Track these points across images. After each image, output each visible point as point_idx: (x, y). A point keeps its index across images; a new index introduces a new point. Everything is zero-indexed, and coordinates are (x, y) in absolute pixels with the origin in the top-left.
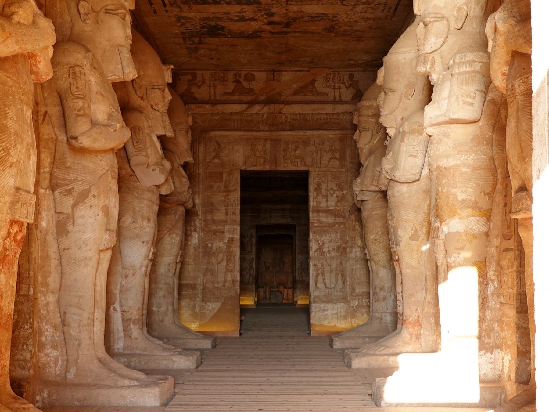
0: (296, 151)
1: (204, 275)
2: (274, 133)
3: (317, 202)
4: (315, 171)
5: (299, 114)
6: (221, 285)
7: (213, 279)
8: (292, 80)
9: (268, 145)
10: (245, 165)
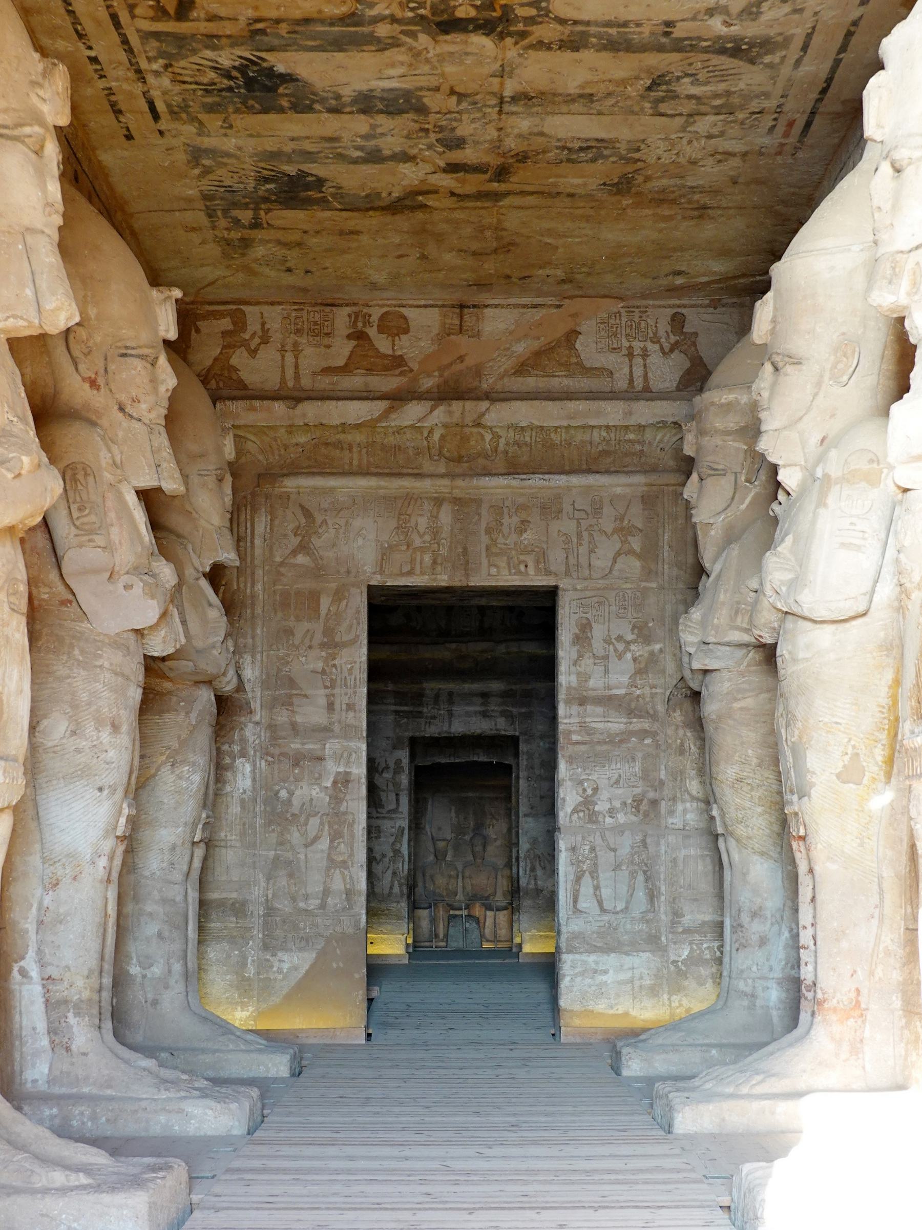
1: (269, 879)
2: (460, 482)
4: (576, 590)
5: (531, 427)
8: (511, 333)
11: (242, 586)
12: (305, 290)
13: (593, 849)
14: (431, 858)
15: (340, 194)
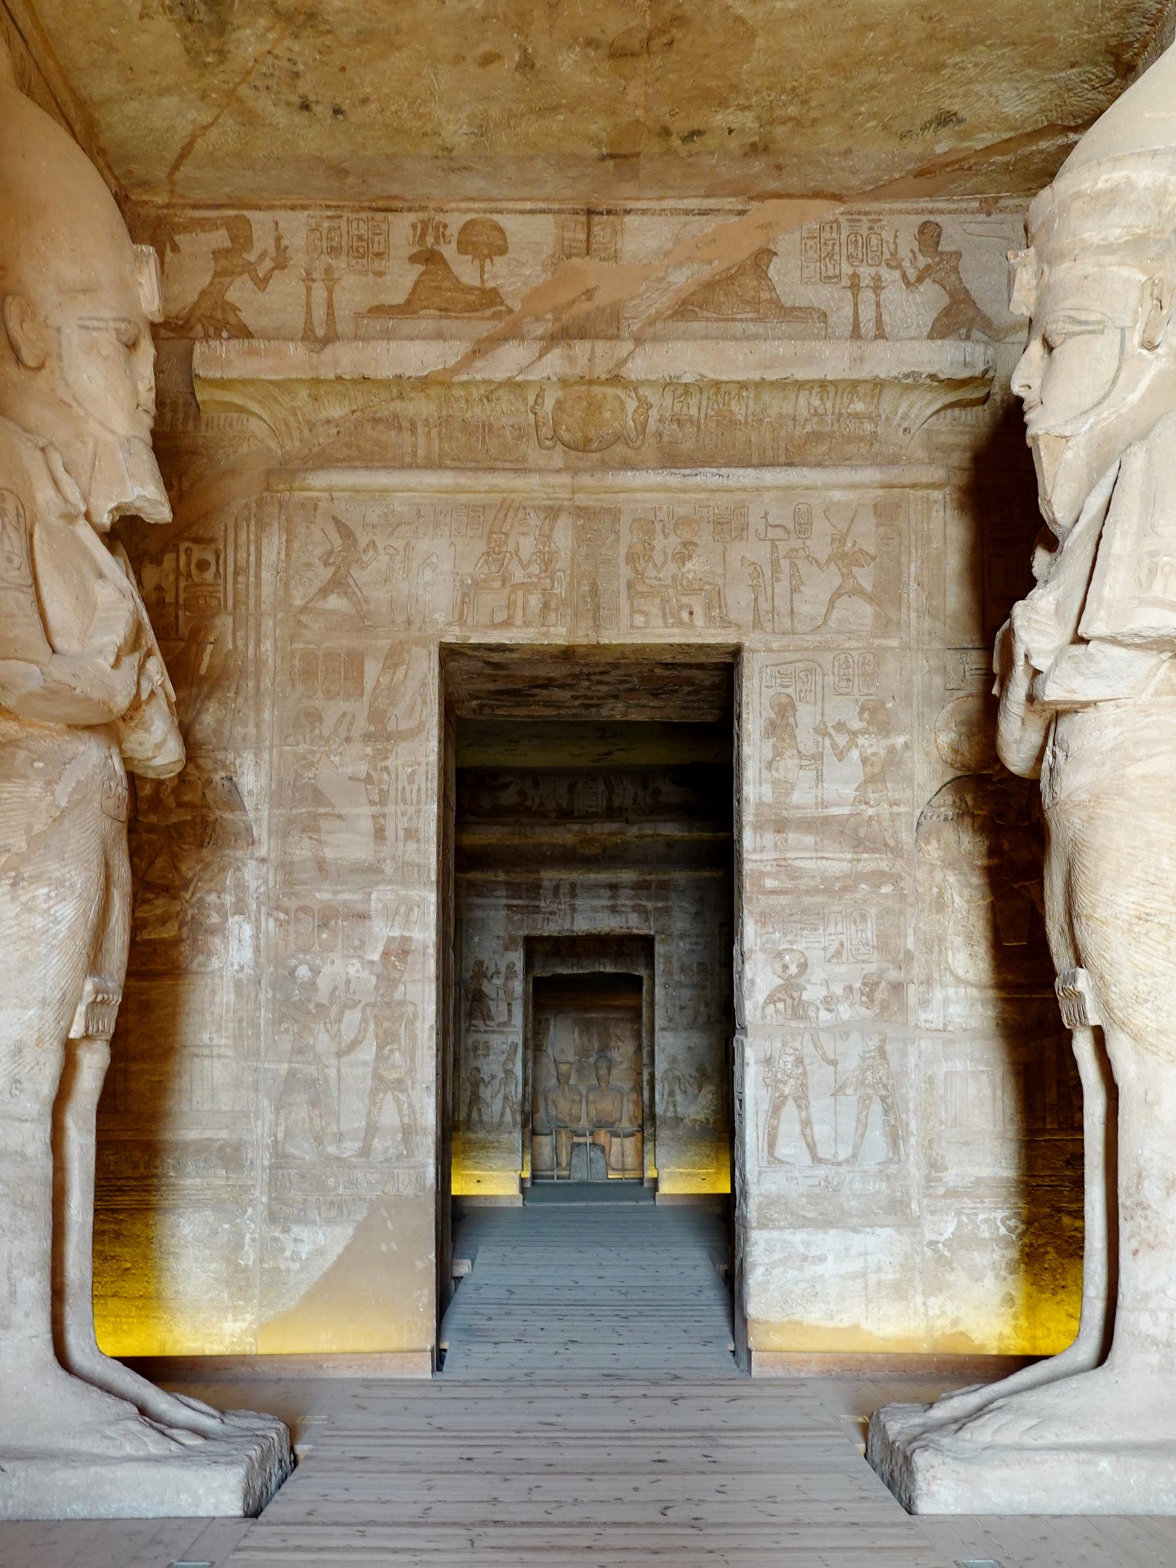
0: (683, 559)
2: (586, 480)
3: (775, 783)
4: (770, 650)
7: (318, 1123)
8: (667, 254)
9: (563, 535)
10: (461, 621)
11: (240, 643)
12: (338, 171)
13: (799, 1061)
14: (553, 1082)
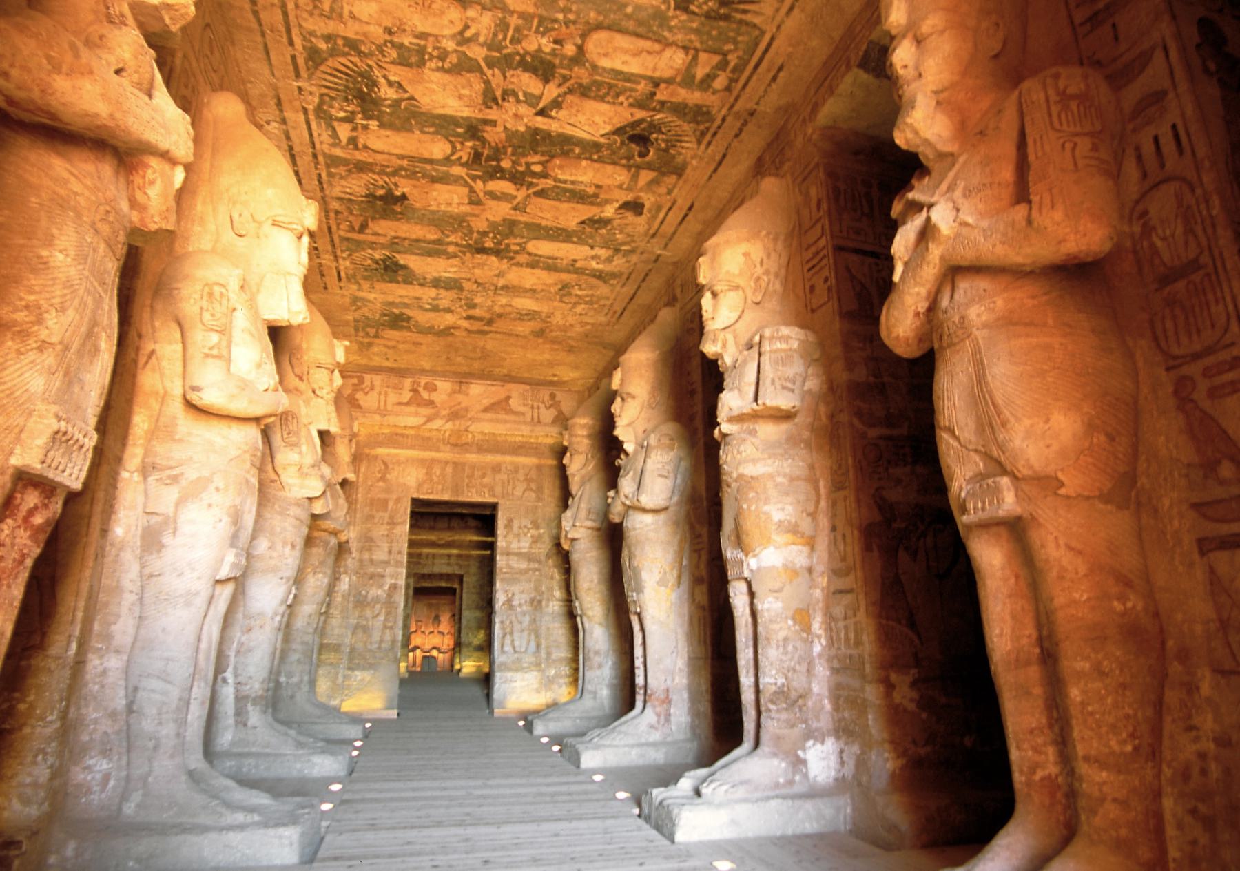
6: (375, 646)
9: (449, 469)
15: (417, 325)
